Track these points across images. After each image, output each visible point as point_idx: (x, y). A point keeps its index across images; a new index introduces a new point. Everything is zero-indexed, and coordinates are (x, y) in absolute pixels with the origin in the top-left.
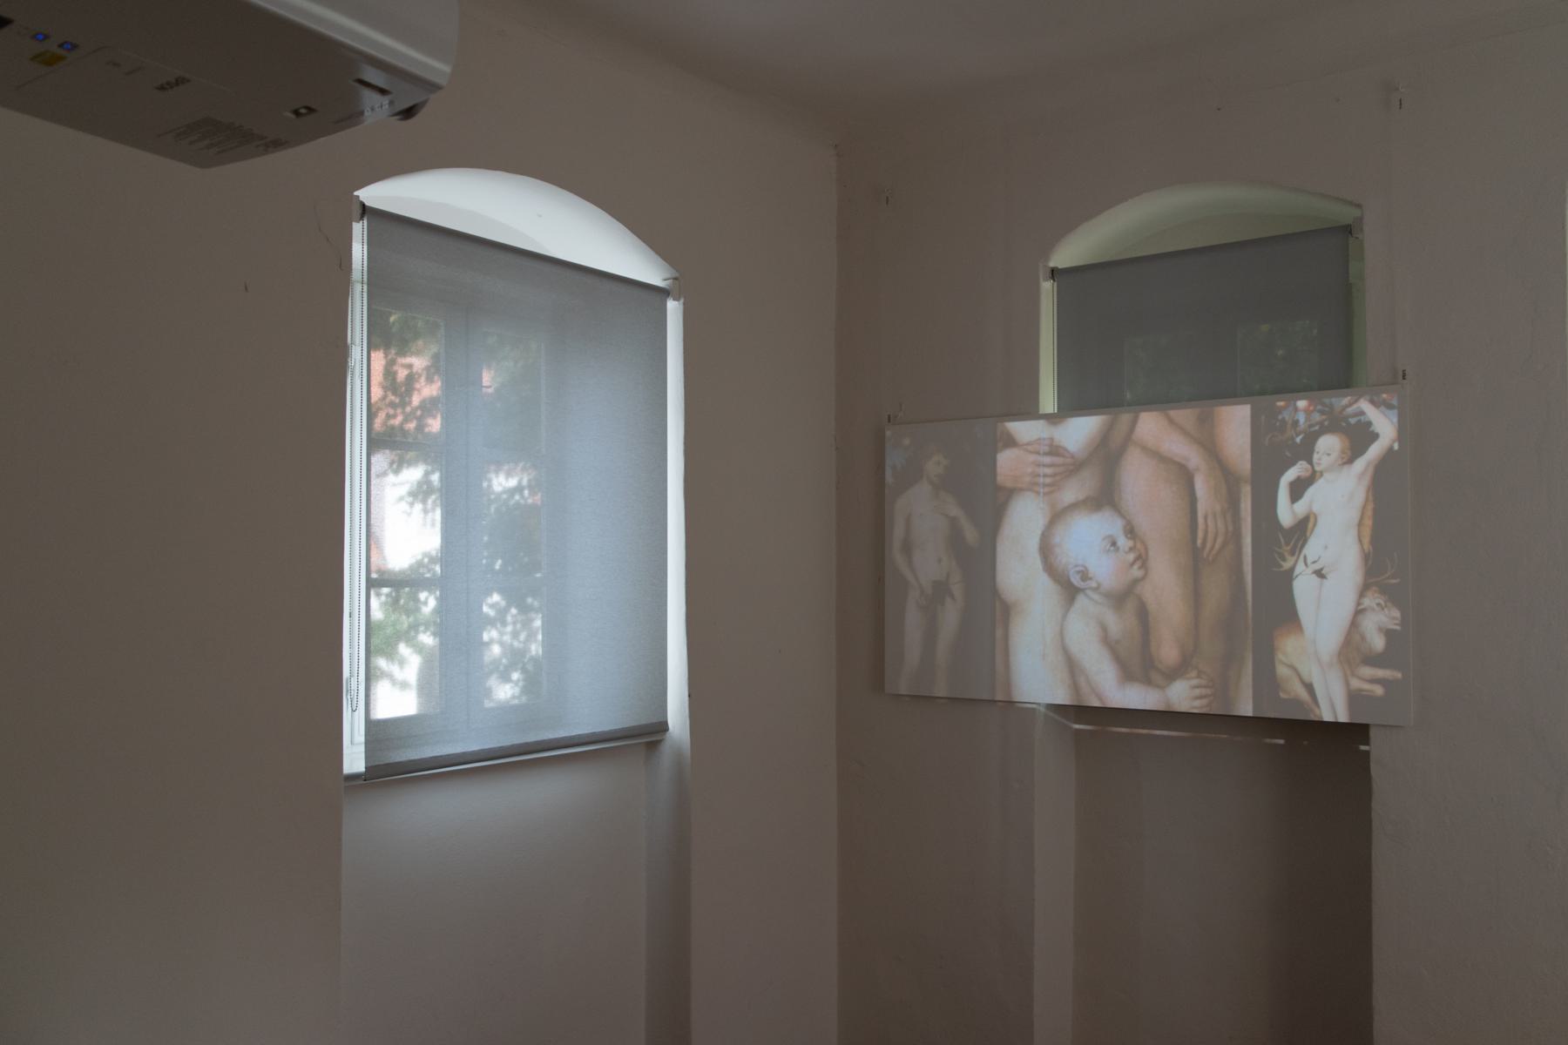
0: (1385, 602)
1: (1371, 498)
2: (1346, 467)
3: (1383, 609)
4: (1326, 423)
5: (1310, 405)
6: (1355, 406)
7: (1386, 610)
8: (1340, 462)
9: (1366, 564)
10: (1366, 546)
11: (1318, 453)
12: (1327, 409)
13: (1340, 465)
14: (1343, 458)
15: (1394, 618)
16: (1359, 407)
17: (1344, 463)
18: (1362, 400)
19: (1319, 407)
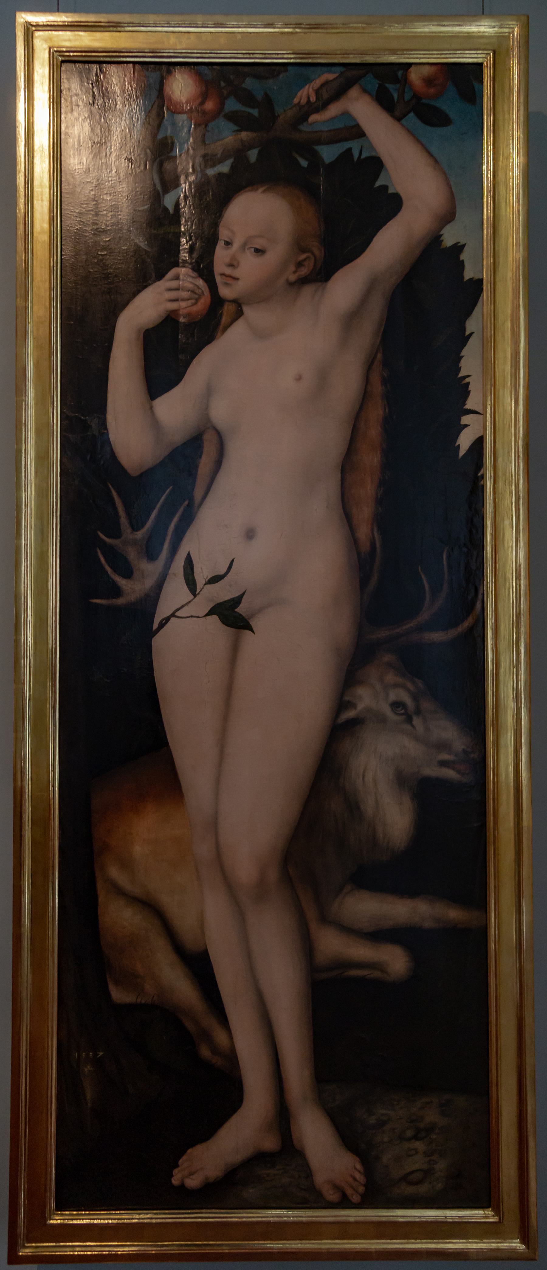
0: (415, 697)
1: (378, 388)
2: (308, 290)
3: (409, 720)
4: (253, 155)
5: (204, 97)
6: (334, 110)
7: (416, 721)
8: (293, 278)
9: (363, 582)
10: (364, 531)
11: (228, 243)
12: (255, 112)
13: (291, 284)
14: (299, 264)
15: (442, 746)
16: (346, 114)
17: (303, 281)
18: (354, 92)
19: (232, 105)
